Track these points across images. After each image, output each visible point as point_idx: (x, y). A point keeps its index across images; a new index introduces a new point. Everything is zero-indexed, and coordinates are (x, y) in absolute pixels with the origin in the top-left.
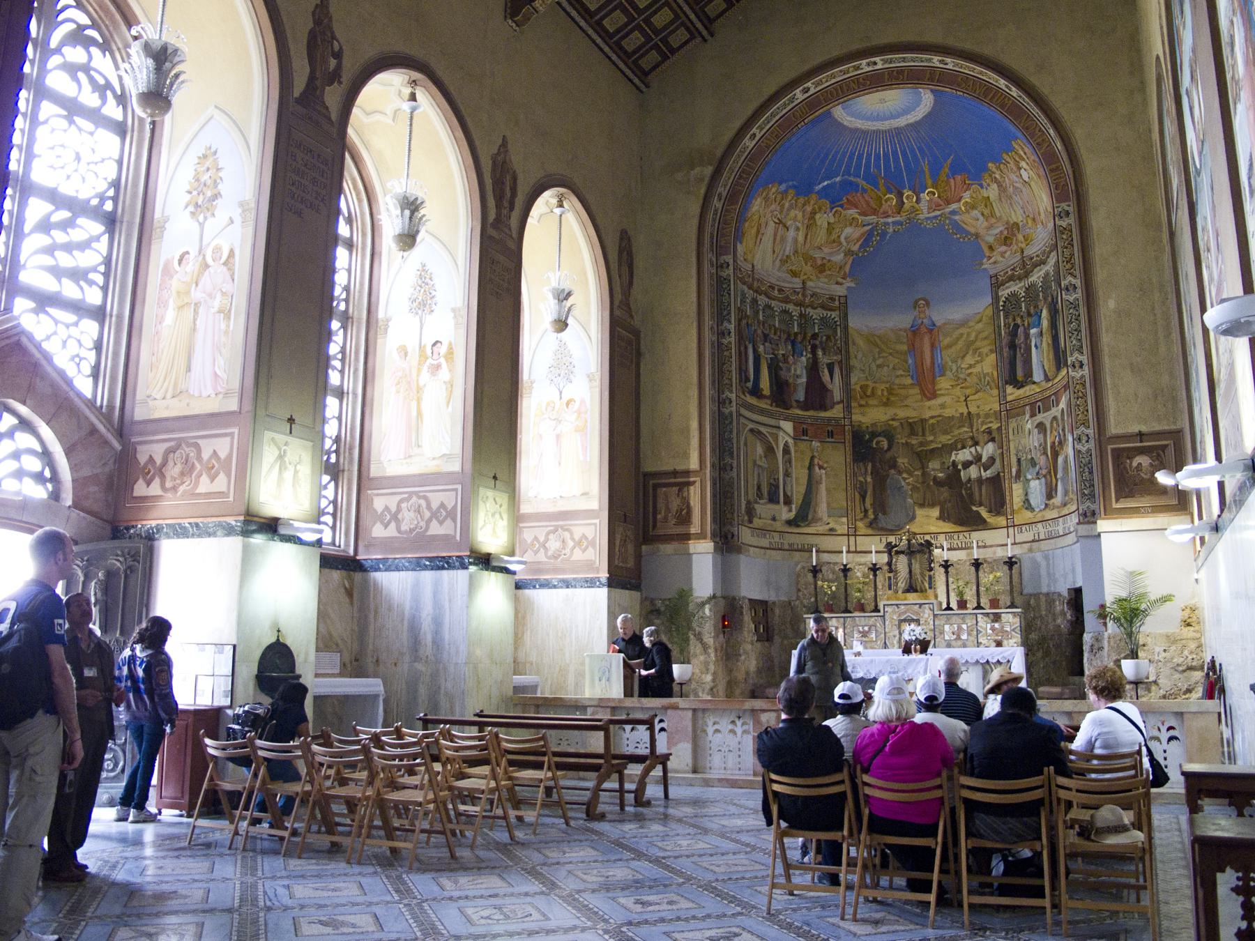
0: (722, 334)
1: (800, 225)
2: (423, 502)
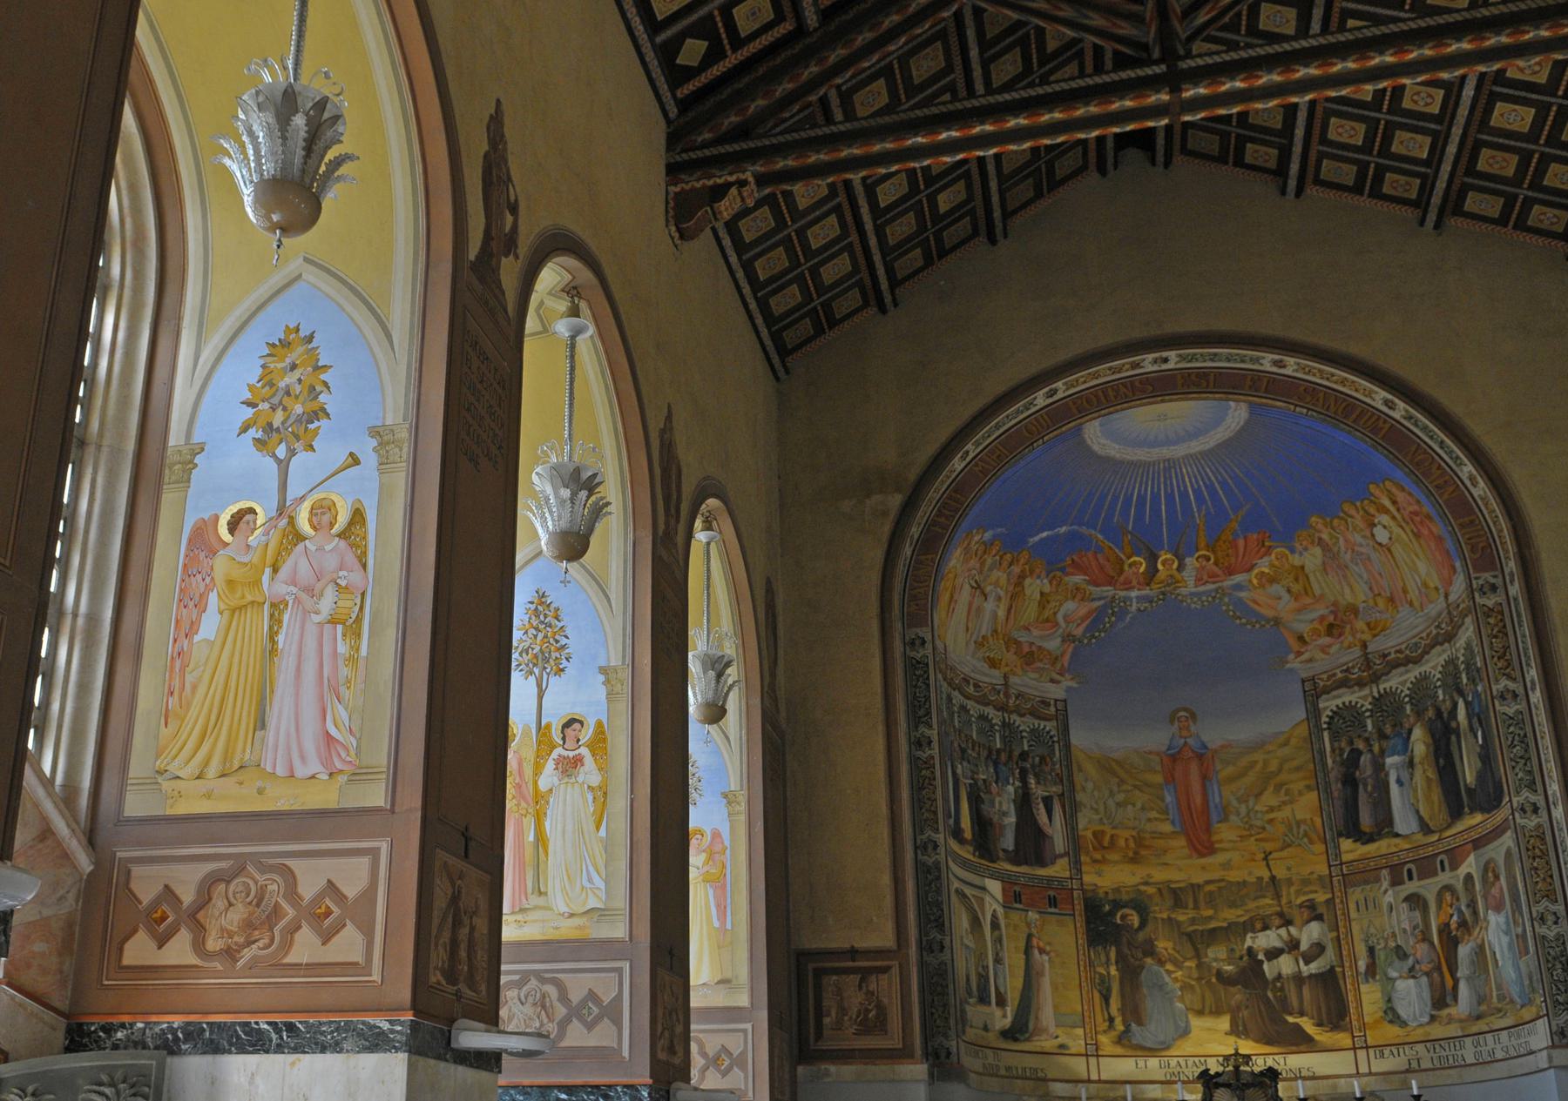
2: (552, 991)
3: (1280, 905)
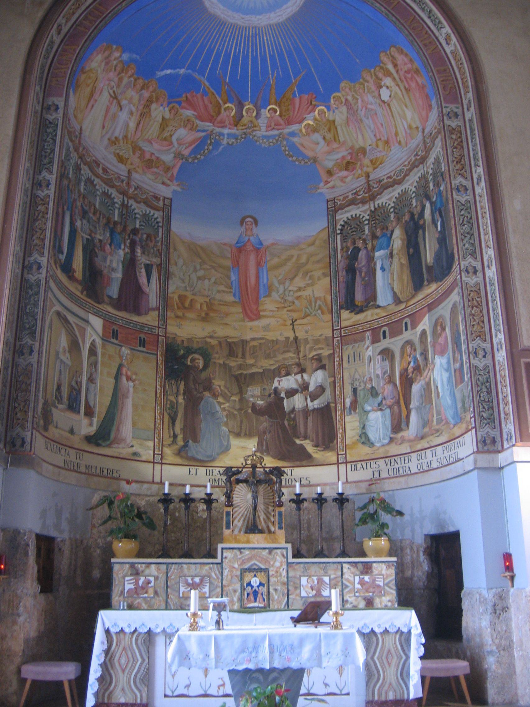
0: (37, 184)
1: (134, 109)
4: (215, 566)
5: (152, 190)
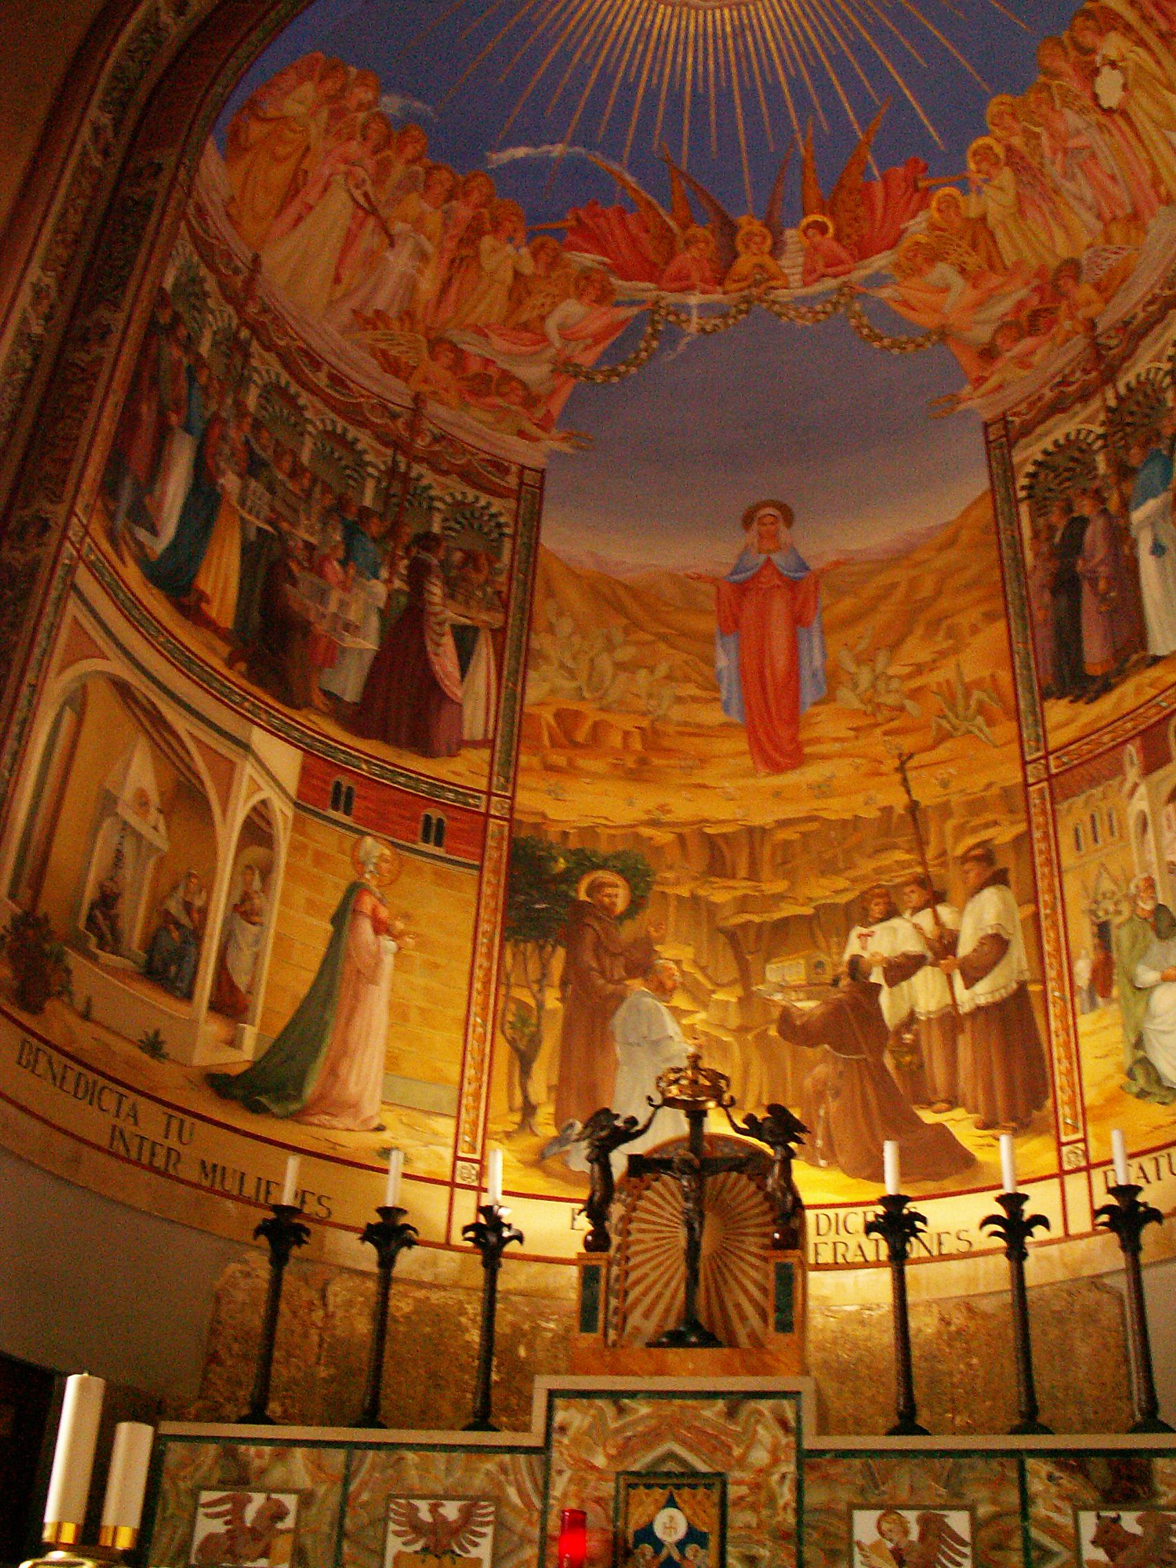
1: (429, 248)
3: (923, 863)
4: (522, 1458)
5: (486, 447)
